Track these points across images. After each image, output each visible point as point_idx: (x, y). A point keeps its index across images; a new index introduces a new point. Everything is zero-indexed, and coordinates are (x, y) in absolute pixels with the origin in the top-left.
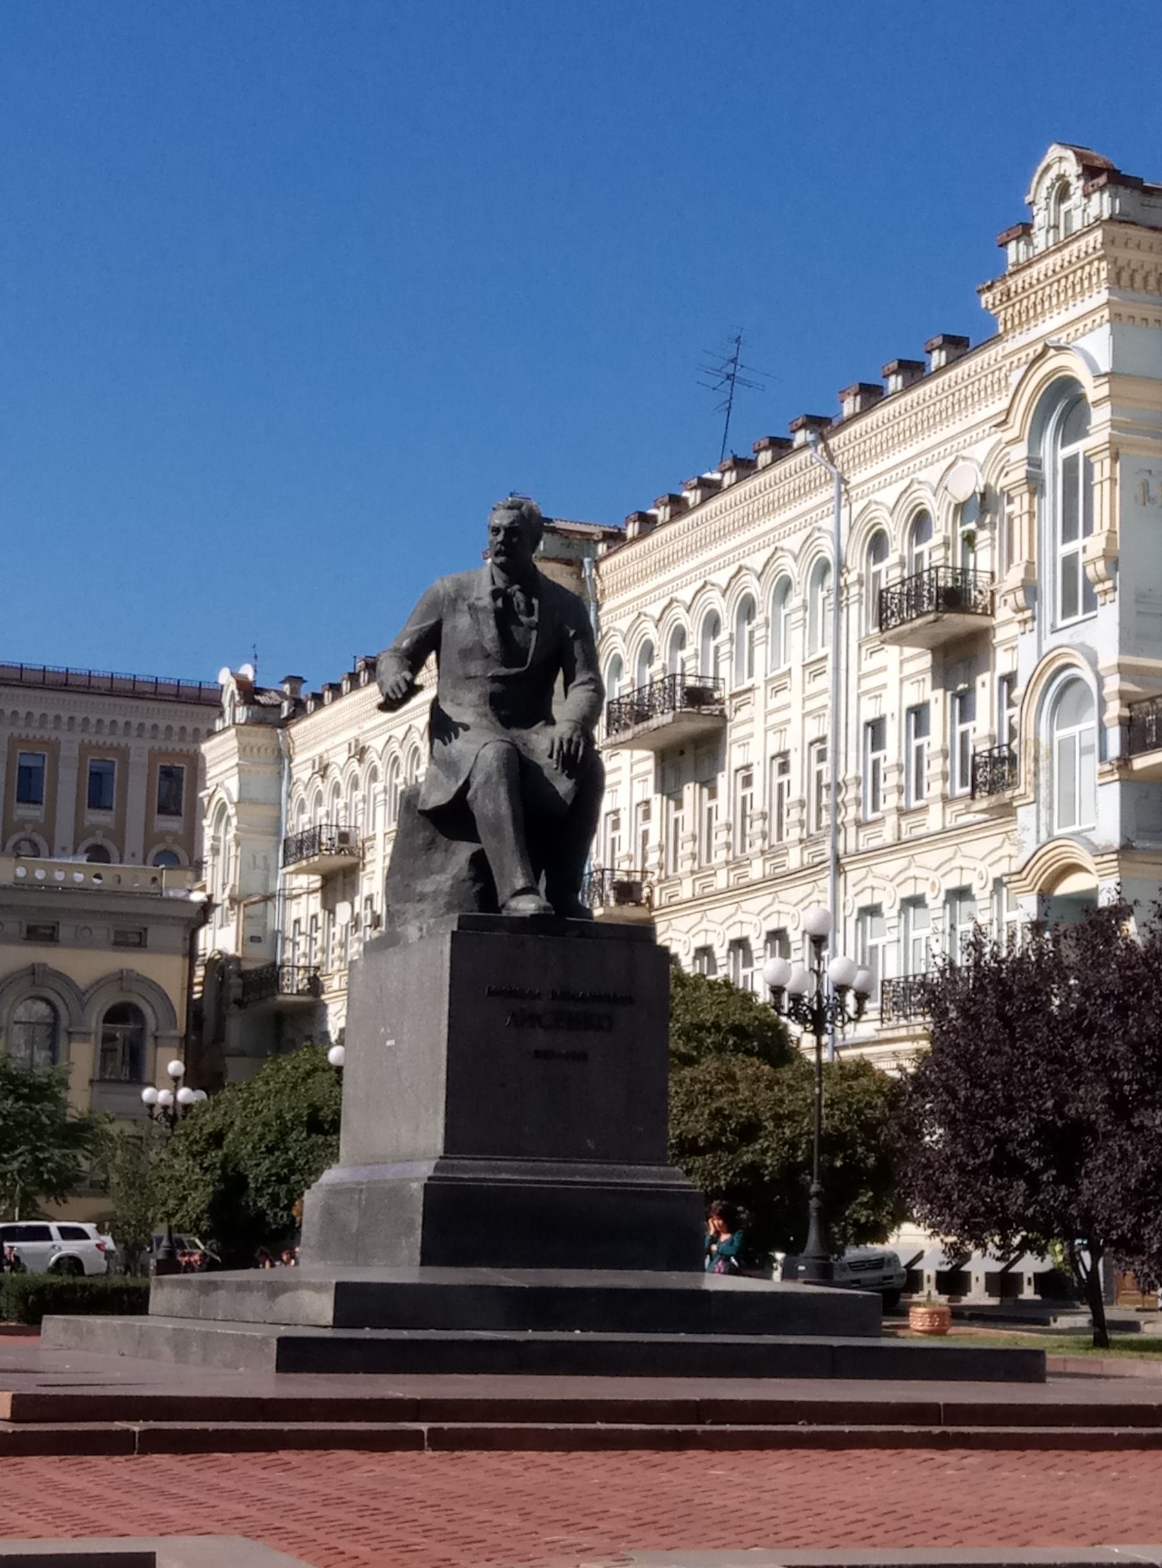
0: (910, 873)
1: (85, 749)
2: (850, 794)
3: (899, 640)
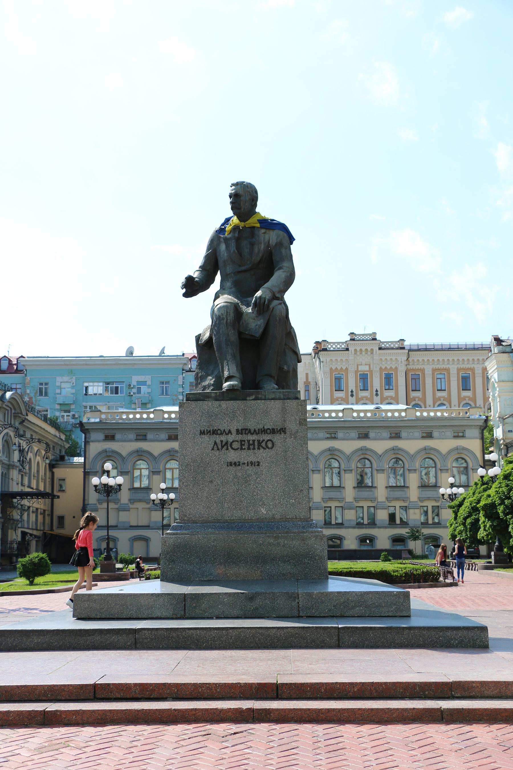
1: (459, 370)
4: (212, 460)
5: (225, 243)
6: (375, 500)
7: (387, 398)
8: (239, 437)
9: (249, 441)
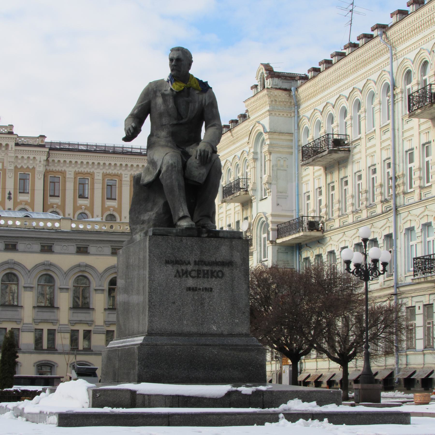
0: (425, 213)
2: (399, 182)
3: (417, 116)
4: (175, 285)
5: (163, 98)
6: (20, 322)
7: (21, 203)
8: (196, 268)
9: (204, 271)
